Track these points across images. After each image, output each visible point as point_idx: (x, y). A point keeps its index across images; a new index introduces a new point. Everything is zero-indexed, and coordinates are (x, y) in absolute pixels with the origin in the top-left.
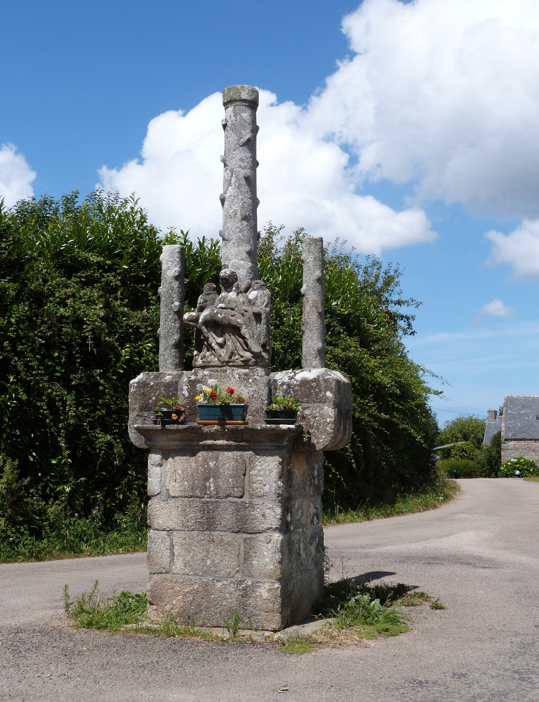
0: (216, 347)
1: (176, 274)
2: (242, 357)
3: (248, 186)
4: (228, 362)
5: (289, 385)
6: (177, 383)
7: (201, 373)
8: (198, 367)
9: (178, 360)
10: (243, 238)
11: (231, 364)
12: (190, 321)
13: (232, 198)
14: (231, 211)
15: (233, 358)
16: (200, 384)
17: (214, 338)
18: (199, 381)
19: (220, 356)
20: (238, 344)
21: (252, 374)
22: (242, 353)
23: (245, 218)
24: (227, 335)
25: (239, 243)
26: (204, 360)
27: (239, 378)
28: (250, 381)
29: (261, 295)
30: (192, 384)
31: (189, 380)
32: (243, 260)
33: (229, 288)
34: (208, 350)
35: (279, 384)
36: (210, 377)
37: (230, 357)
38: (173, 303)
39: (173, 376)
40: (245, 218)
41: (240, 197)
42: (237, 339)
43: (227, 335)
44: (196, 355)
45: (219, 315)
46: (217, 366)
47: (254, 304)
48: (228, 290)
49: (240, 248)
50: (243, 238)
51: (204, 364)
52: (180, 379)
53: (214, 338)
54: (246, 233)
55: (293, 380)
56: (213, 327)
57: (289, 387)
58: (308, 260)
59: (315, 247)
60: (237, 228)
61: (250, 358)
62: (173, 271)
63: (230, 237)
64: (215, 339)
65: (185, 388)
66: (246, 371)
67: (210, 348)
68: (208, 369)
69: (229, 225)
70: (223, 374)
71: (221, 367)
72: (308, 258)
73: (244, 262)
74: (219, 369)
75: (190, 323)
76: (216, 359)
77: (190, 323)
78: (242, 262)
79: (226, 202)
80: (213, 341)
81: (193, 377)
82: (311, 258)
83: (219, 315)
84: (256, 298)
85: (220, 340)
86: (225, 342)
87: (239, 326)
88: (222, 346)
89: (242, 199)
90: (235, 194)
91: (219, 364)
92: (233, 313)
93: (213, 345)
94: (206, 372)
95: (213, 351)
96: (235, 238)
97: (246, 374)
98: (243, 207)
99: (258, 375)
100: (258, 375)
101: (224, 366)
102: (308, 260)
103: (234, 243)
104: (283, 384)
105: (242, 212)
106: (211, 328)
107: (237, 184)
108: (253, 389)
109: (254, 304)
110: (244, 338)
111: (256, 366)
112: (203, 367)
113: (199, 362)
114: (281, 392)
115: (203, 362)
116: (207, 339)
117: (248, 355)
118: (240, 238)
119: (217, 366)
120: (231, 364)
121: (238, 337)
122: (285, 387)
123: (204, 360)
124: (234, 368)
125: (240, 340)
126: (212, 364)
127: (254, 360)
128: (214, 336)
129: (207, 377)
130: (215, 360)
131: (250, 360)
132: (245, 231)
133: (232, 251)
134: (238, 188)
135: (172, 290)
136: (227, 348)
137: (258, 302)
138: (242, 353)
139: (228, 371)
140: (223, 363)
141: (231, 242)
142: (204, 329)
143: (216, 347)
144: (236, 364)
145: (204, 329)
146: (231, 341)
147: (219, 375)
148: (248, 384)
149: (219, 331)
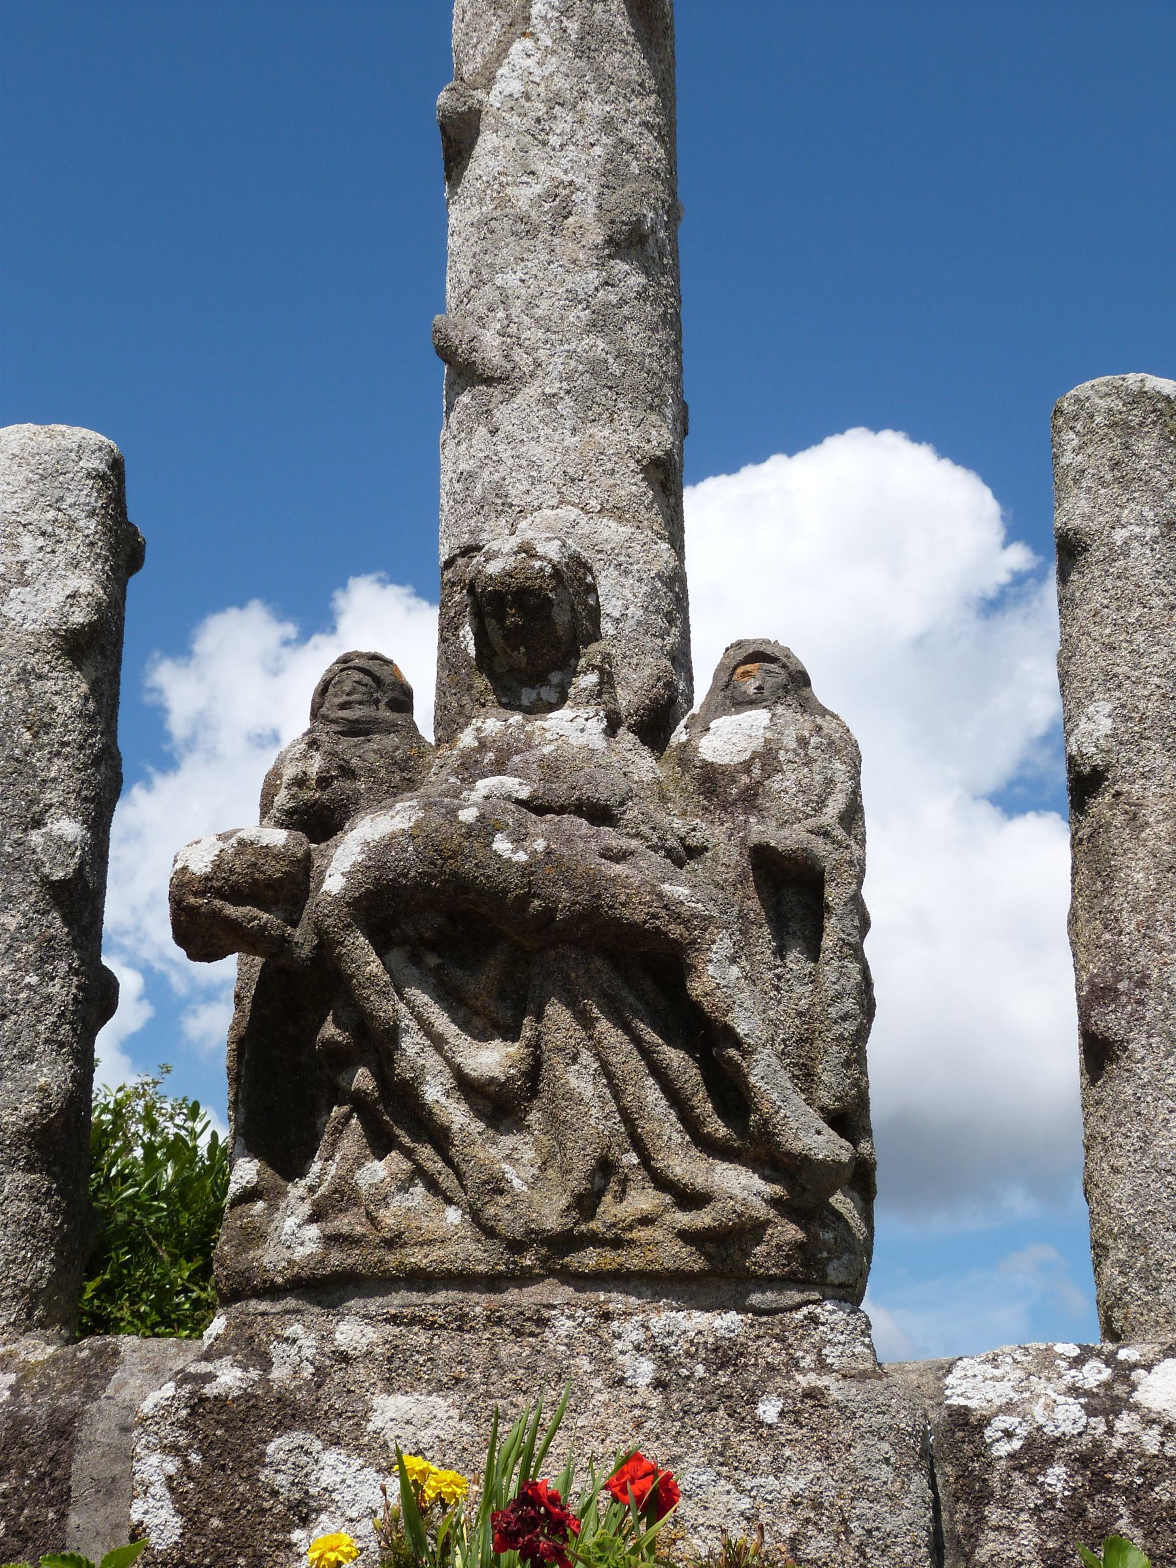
0: (456, 1115)
1: (79, 617)
2: (690, 1198)
3: (646, 55)
4: (564, 1242)
5: (1094, 1466)
6: (64, 1429)
7: (298, 1342)
8: (272, 1292)
9: (44, 1265)
10: (616, 368)
11: (589, 1259)
12: (236, 896)
13: (541, 109)
14: (524, 196)
15: (611, 1210)
16: (298, 1437)
17: (438, 1042)
18: (289, 1413)
19: (497, 1187)
20: (653, 1095)
21: (772, 1353)
22: (686, 1165)
23: (628, 242)
24: (558, 1013)
25: (585, 400)
26: (344, 1223)
27: (660, 1384)
28: (769, 1410)
29: (803, 742)
30: (223, 1436)
31: (198, 1404)
32: (617, 512)
33: (537, 679)
34: (380, 1145)
35: (1002, 1449)
36: (396, 1371)
37: (585, 1204)
38: (38, 823)
39: (26, 1372)
40: (628, 242)
41: (595, 108)
42: (646, 1052)
43: (558, 1013)
44: (249, 1195)
45: (502, 845)
46: (464, 1280)
47: (750, 800)
48: (527, 696)
49: (601, 432)
50: (616, 368)
51: (337, 1259)
52: (91, 1394)
53: (438, 1042)
54: (634, 337)
55: (1126, 1423)
56: (433, 947)
57: (1101, 1484)
58: (1120, 535)
59: (1161, 452)
60: (574, 299)
61: (762, 1210)
62: (55, 596)
63: (519, 355)
64: (446, 1053)
65: (154, 1466)
66: (727, 1323)
67: (397, 1117)
68: (374, 1305)
69: (509, 279)
70: (508, 1350)
71: (493, 1282)
72: (1117, 523)
73: (626, 530)
74: (479, 1303)
75: (233, 911)
76: (453, 1215)
77: (233, 911)
78: (612, 531)
79: (487, 141)
80: (432, 1061)
81: (229, 1378)
82: (1141, 520)
83: (502, 845)
84: (767, 758)
85: (491, 1059)
86: (534, 1071)
87: (676, 931)
88: (499, 1105)
89: (608, 125)
90: (559, 83)
91: (477, 1255)
92: (610, 837)
93: (434, 1092)
94: (352, 1333)
95: (426, 1153)
96: (557, 366)
97: (724, 1355)
98: (613, 173)
99: (822, 1366)
100: (822, 1366)
101: (524, 1278)
102: (1120, 535)
103: (549, 400)
104: (1037, 1452)
105: (612, 198)
106: (415, 960)
107: (573, 26)
108: (794, 1484)
109: (750, 800)
110: (706, 1035)
111: (801, 1283)
112: (323, 1289)
113: (293, 1236)
114: (1026, 1525)
115: (332, 1240)
116: (378, 1043)
117: (739, 1186)
118: (596, 369)
119: (464, 1280)
120: (589, 1259)
121: (650, 1036)
122: (1056, 1477)
123: (344, 1223)
124: (617, 1301)
125: (674, 1057)
126: (418, 1257)
127: (791, 1232)
128: (442, 1021)
129: (360, 1371)
130: (444, 1229)
131: (754, 1230)
132: (631, 329)
133: (535, 451)
134: (582, 51)
135: (39, 728)
136: (552, 1119)
137: (785, 782)
138: (686, 1165)
139: (564, 1326)
140: (516, 1246)
141: (531, 391)
142: (365, 960)
143: (456, 1115)
144: (633, 1260)
145: (365, 960)
146: (591, 1065)
147: (478, 1355)
148: (743, 1443)
149: (480, 985)
